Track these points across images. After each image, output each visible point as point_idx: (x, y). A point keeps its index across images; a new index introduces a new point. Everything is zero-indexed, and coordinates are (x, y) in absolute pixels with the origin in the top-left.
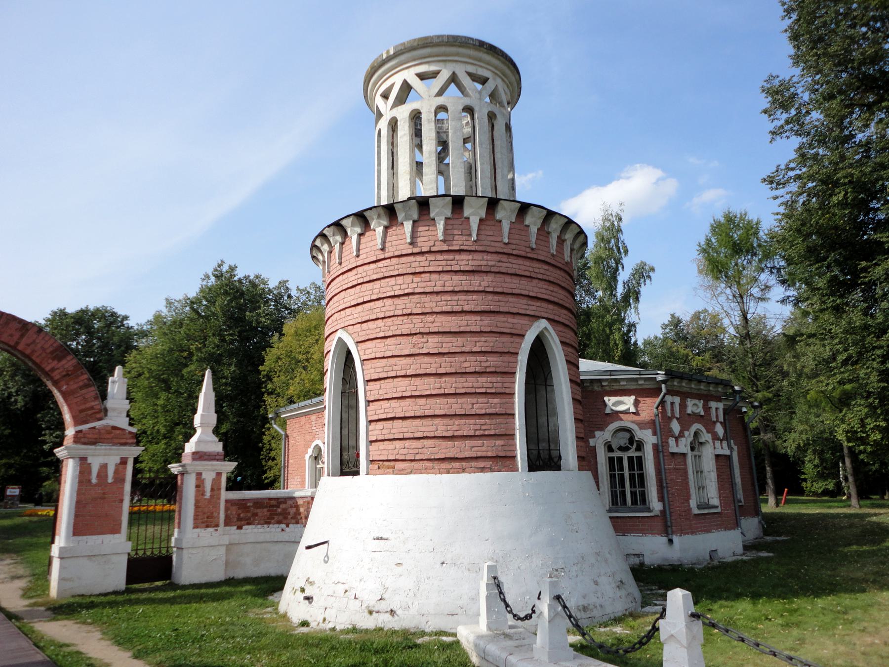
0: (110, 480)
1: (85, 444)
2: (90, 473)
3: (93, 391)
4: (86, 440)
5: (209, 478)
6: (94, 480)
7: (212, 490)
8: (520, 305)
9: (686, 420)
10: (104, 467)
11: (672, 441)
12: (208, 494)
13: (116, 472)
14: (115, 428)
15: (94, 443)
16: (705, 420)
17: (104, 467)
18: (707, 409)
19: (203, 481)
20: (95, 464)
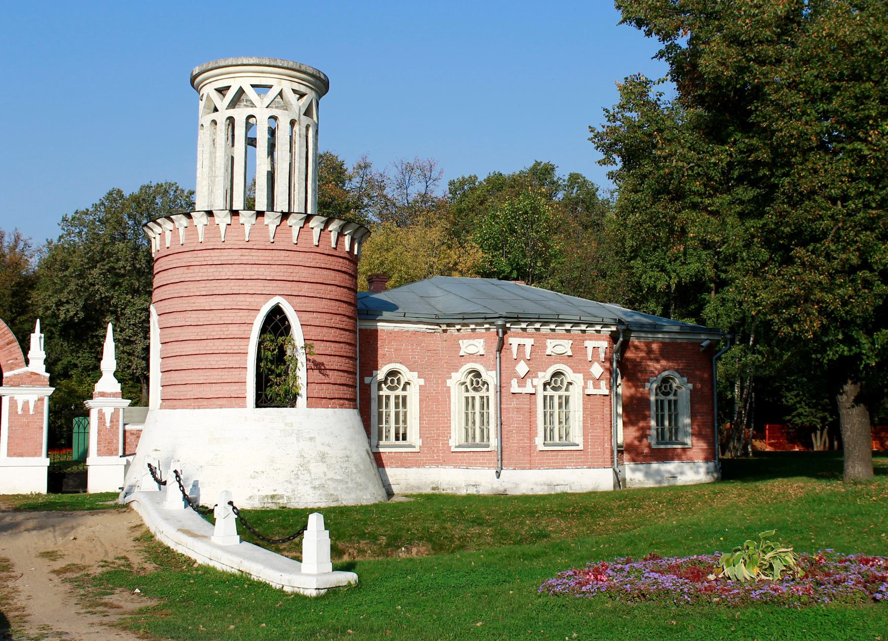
0: (31, 412)
1: (12, 386)
2: (17, 407)
3: (16, 347)
4: (11, 383)
5: (108, 412)
6: (20, 412)
7: (111, 421)
8: (257, 287)
9: (536, 362)
10: (26, 403)
11: (514, 382)
12: (108, 424)
13: (36, 407)
14: (32, 373)
15: (18, 385)
16: (576, 360)
17: (26, 403)
18: (578, 348)
19: (104, 415)
20: (20, 400)
